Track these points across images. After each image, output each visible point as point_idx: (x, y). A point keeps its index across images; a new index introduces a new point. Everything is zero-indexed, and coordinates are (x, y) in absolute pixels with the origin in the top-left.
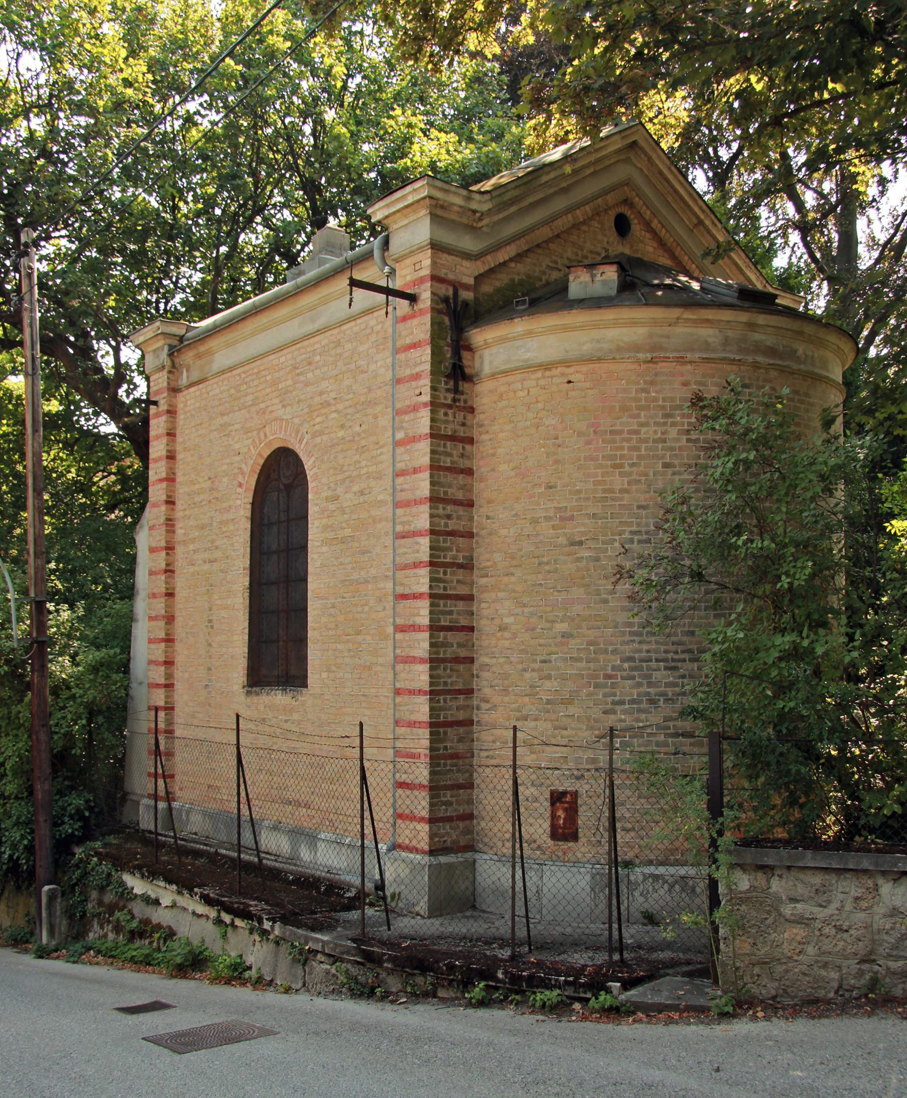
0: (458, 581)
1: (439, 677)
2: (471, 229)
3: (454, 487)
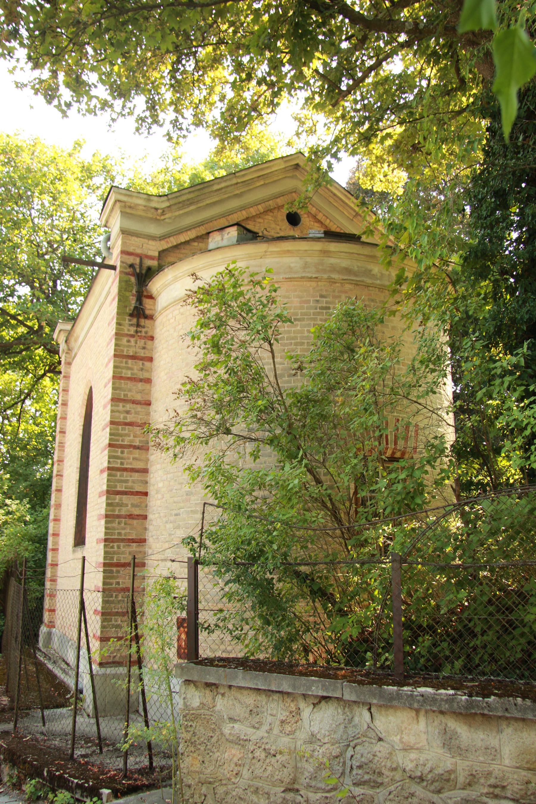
0: (134, 459)
1: (114, 529)
2: (156, 220)
3: (134, 391)
